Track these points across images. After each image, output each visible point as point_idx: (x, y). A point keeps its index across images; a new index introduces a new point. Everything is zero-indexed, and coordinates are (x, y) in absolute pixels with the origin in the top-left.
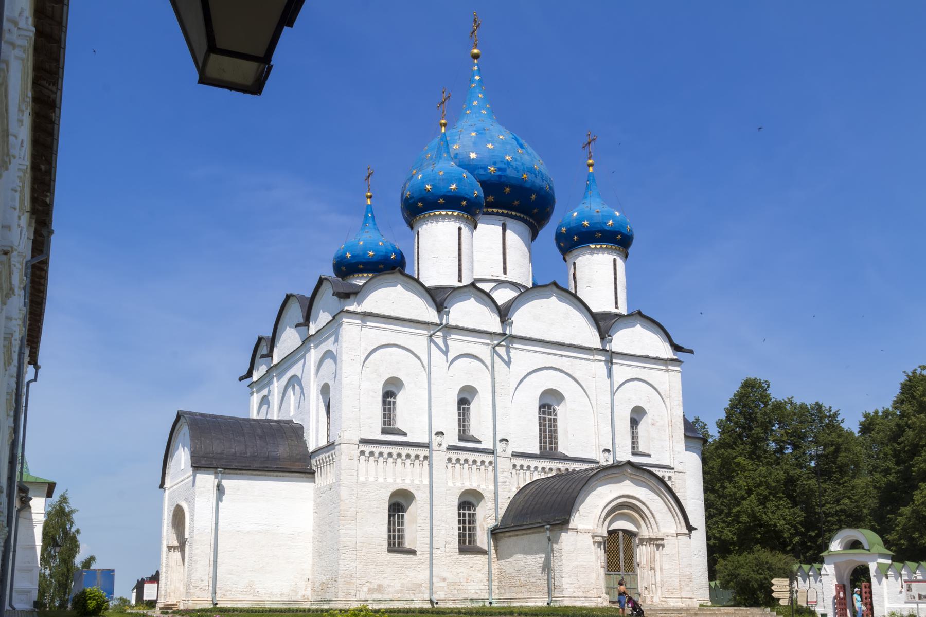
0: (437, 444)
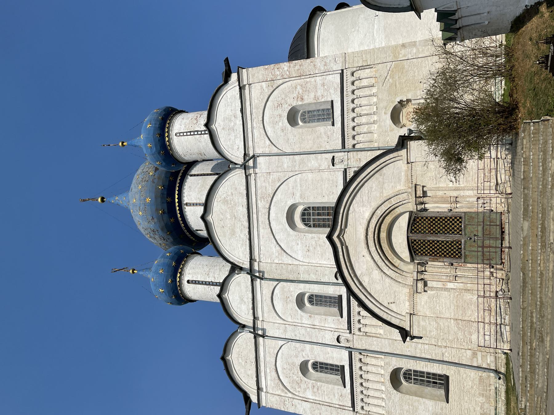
0: (347, 343)
